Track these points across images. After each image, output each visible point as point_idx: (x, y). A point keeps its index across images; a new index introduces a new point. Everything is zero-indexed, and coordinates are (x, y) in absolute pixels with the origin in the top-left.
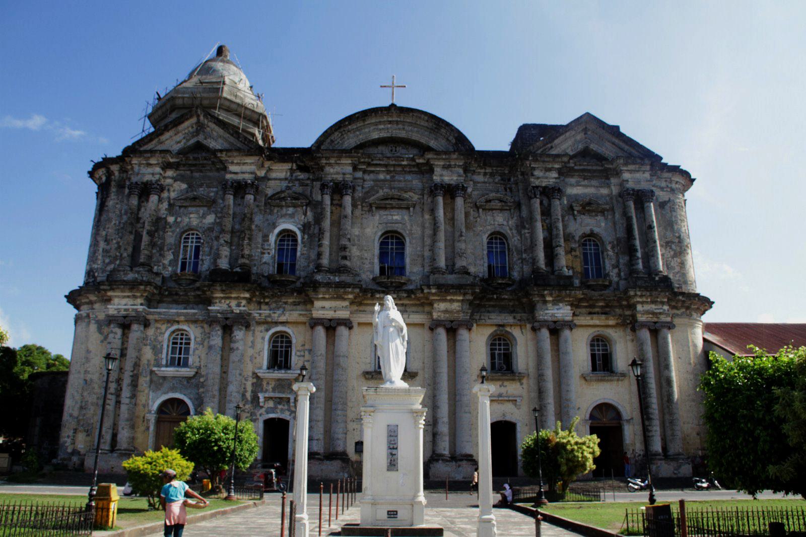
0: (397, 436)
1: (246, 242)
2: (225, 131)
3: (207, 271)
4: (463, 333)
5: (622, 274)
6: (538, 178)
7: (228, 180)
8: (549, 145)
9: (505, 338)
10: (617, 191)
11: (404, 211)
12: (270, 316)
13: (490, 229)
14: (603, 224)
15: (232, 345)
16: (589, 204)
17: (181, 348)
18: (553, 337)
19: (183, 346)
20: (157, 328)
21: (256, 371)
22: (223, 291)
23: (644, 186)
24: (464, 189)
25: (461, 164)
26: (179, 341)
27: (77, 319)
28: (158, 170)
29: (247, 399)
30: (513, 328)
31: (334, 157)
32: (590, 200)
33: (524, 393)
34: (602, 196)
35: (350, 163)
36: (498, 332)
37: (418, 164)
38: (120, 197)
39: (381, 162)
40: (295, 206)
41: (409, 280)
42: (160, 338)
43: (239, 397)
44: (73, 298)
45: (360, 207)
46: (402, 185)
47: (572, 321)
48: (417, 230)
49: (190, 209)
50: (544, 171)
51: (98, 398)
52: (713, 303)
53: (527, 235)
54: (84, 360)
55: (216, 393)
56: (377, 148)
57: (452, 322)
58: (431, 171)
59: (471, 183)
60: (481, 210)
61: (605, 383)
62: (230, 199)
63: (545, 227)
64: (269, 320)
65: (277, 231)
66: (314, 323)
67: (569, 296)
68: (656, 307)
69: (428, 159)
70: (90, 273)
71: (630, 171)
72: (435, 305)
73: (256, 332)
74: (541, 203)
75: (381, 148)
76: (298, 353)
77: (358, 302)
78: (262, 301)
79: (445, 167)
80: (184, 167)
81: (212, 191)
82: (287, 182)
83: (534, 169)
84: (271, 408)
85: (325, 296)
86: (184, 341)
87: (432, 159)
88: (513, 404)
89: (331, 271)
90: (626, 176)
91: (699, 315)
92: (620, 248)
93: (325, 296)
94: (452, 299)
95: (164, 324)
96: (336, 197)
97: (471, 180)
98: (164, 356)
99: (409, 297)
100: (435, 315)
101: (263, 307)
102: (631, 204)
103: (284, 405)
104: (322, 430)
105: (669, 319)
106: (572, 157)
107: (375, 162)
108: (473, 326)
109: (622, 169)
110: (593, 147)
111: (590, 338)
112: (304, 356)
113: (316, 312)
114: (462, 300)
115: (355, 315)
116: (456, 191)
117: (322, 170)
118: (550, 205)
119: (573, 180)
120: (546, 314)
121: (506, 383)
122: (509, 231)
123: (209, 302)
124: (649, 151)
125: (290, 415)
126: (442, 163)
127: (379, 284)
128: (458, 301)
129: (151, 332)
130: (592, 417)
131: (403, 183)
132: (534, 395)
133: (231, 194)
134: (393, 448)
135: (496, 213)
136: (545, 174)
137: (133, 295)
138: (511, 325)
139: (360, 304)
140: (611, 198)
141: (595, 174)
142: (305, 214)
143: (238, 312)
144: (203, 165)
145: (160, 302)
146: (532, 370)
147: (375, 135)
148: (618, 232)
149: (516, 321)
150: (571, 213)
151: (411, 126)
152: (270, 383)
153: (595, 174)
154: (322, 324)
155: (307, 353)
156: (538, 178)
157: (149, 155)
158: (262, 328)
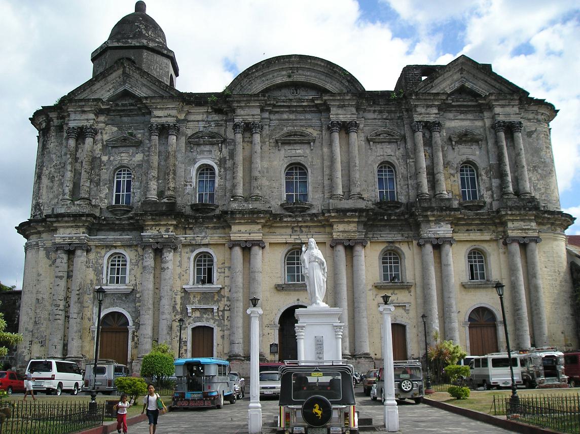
0: (322, 344)
1: (171, 176)
2: (148, 80)
3: (138, 202)
4: (359, 249)
5: (495, 195)
6: (421, 114)
7: (154, 123)
8: (430, 85)
9: (395, 253)
10: (490, 124)
11: (306, 146)
12: (194, 239)
13: (380, 160)
14: (478, 153)
15: (163, 265)
16: (466, 135)
17: (118, 269)
18: (436, 251)
19: (120, 267)
20: (97, 253)
21: (184, 287)
22: (153, 220)
23: (514, 119)
24: (357, 125)
25: (353, 103)
26: (117, 263)
27: (27, 247)
28: (92, 116)
29: (177, 311)
30: (401, 244)
31: (244, 101)
32: (466, 131)
33: (412, 300)
34: (476, 128)
36: (389, 248)
37: (316, 106)
38: (59, 141)
39: (285, 104)
40: (212, 144)
41: (311, 205)
42: (100, 261)
43: (171, 310)
44: (23, 229)
45: (267, 143)
46: (303, 123)
47: (452, 238)
48: (317, 162)
49: (122, 149)
50: (425, 108)
51: (49, 314)
52: (575, 219)
53: (412, 164)
54: (35, 282)
55: (151, 306)
56: (281, 91)
57: (349, 240)
58: (328, 110)
59: (363, 119)
60: (371, 143)
61: (481, 290)
62: (155, 138)
63: (428, 157)
64: (194, 242)
65: (197, 165)
66: (233, 244)
67: (450, 216)
68: (525, 224)
69: (326, 100)
70: (37, 207)
71: (503, 106)
72: (335, 227)
73: (183, 253)
74: (424, 136)
75: (284, 91)
76: (219, 270)
77: (269, 225)
78: (187, 226)
80: (114, 112)
81: (140, 133)
82: (204, 123)
83: (416, 106)
84: (198, 317)
85: (240, 221)
86: (121, 263)
87: (328, 100)
88: (403, 309)
89: (246, 200)
90: (497, 110)
91: (563, 230)
92: (493, 173)
93: (240, 221)
94: (349, 221)
96: (247, 135)
97: (362, 117)
98: (104, 276)
99: (312, 220)
100: (335, 236)
101: (188, 232)
102: (502, 135)
103: (209, 315)
104: (241, 335)
105: (536, 234)
106: (449, 95)
107: (279, 104)
108: (367, 243)
109: (494, 104)
110: (467, 85)
111: (468, 252)
112: (224, 272)
113: (233, 235)
115: (266, 237)
116: (350, 127)
117: (234, 113)
118: (431, 137)
119: (451, 115)
120: (430, 232)
121: (396, 292)
122: (396, 161)
123: (142, 229)
124: (517, 87)
125: (214, 323)
126: (338, 104)
127: (287, 209)
128: (354, 222)
129: (92, 256)
130: (470, 319)
131: (304, 121)
132: (420, 301)
133: (157, 136)
134: (320, 353)
135: (385, 145)
136: (426, 110)
138: (400, 242)
139: (271, 227)
140: (485, 130)
141: (470, 109)
142: (221, 151)
143: (167, 237)
144: (131, 110)
145: (99, 230)
146: (418, 280)
147: (279, 80)
148: (491, 160)
149: (404, 238)
150: (450, 143)
151: (310, 71)
152: (196, 296)
153: (470, 109)
154: (239, 245)
155: (227, 270)
156: (421, 114)
157: (83, 103)
158: (188, 250)
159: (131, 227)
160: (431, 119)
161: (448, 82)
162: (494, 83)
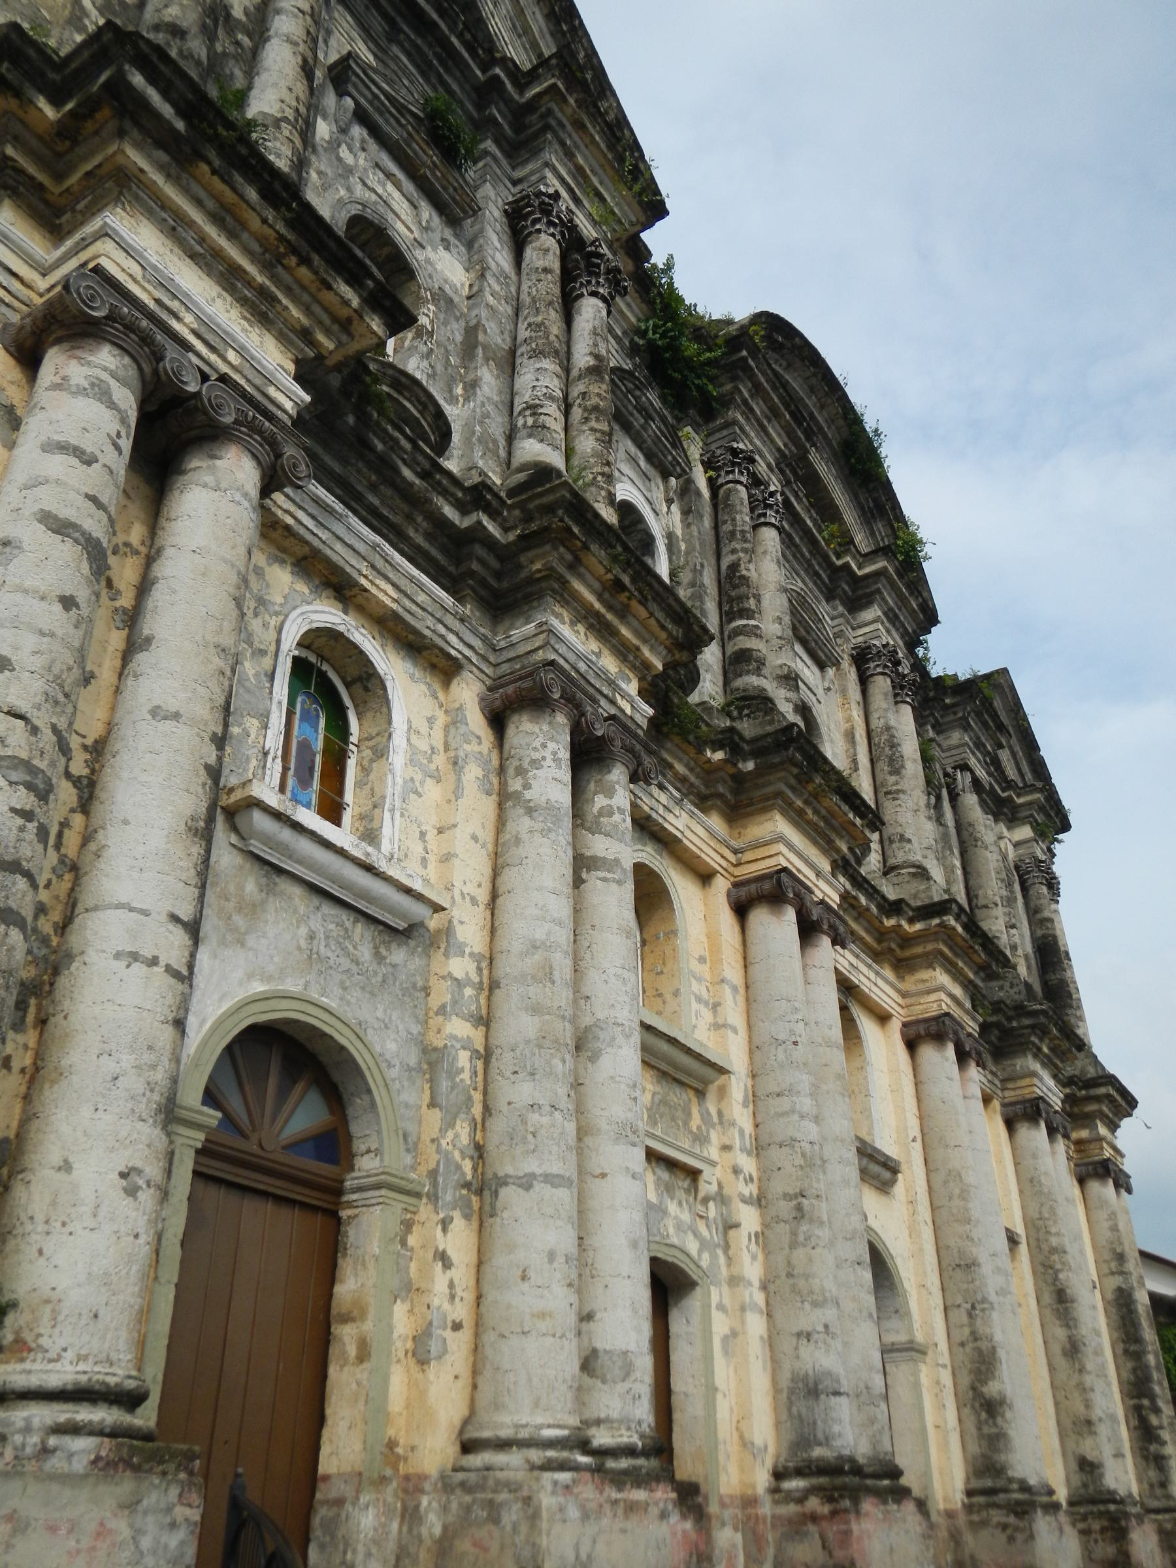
31: (767, 399)
35: (779, 450)
37: (847, 566)
95: (282, 562)
114: (971, 982)
137: (262, 291)
159: (434, 552)
162: (1026, 768)
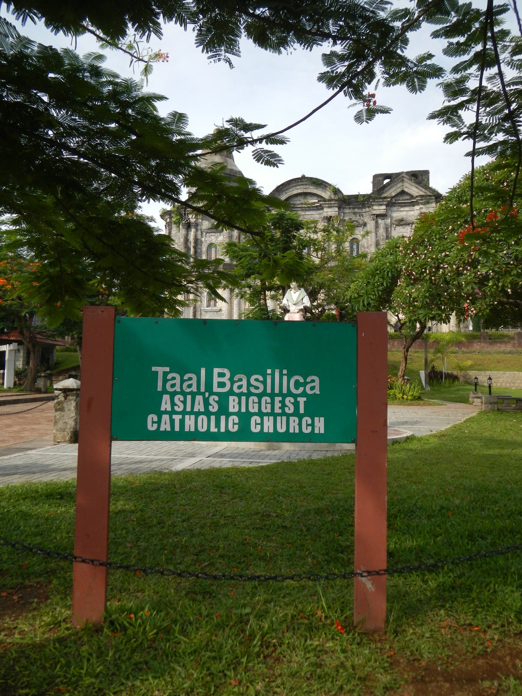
16: (402, 220)
58: (322, 209)
75: (299, 198)
79: (329, 207)
83: (373, 205)
110: (406, 190)
119: (395, 209)
147: (295, 192)
160: (382, 212)
161: (394, 189)
